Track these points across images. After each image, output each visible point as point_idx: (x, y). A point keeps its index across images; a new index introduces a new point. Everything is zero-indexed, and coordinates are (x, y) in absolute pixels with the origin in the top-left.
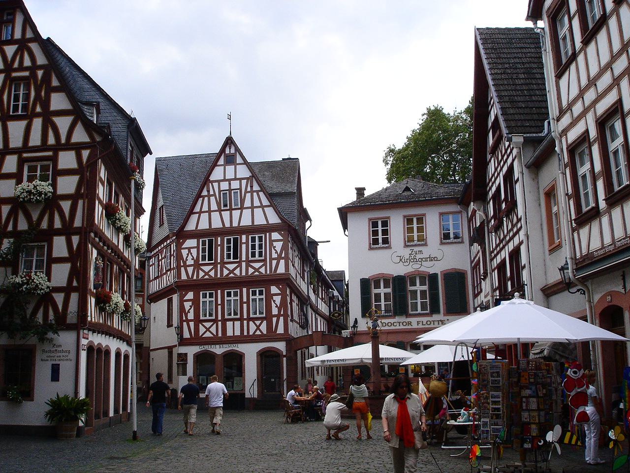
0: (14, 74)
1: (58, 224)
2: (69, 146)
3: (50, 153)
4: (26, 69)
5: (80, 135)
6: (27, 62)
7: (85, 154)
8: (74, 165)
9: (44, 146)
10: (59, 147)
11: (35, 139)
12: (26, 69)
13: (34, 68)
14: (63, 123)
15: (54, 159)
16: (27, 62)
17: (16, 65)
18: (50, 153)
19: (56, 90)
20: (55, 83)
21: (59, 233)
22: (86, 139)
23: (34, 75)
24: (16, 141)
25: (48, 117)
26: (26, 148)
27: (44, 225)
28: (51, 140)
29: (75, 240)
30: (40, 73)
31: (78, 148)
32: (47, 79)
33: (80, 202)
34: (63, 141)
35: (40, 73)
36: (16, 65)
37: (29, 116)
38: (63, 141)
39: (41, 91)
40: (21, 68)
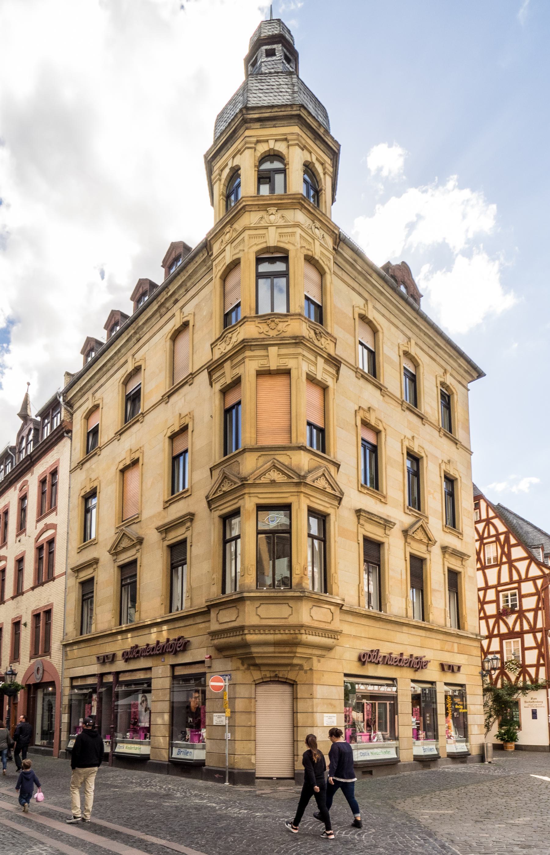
0: (485, 541)
1: (526, 627)
2: (527, 579)
3: (516, 585)
4: (493, 536)
5: (535, 571)
6: (493, 532)
7: (539, 582)
8: (533, 591)
9: (511, 582)
10: (520, 581)
11: (505, 578)
12: (493, 536)
13: (497, 535)
14: (522, 566)
15: (519, 588)
16: (493, 532)
17: (486, 535)
18: (516, 585)
19: (514, 545)
20: (513, 541)
21: (527, 632)
22: (539, 573)
23: (498, 540)
24: (492, 581)
25: (511, 563)
26: (499, 584)
27: (517, 629)
28: (515, 577)
29: (539, 635)
30: (502, 537)
31: (534, 579)
32: (507, 540)
33: (540, 613)
34: (523, 576)
35: (502, 537)
36: (486, 535)
37: (499, 565)
38: (523, 576)
39: (504, 547)
40: (489, 536)
